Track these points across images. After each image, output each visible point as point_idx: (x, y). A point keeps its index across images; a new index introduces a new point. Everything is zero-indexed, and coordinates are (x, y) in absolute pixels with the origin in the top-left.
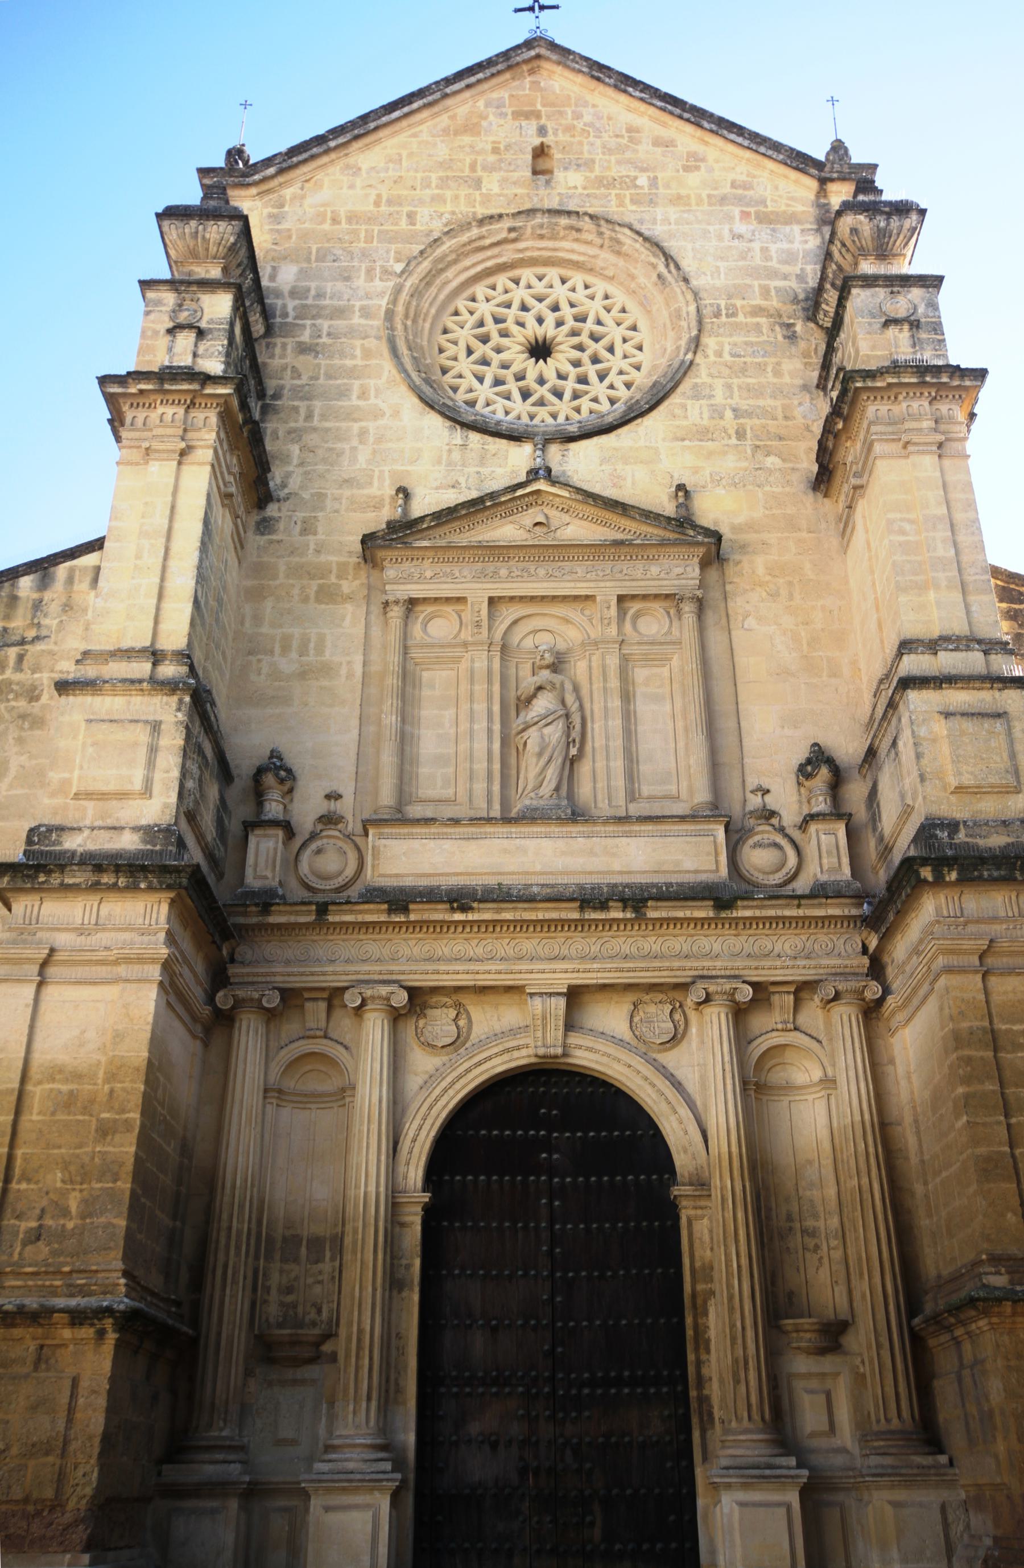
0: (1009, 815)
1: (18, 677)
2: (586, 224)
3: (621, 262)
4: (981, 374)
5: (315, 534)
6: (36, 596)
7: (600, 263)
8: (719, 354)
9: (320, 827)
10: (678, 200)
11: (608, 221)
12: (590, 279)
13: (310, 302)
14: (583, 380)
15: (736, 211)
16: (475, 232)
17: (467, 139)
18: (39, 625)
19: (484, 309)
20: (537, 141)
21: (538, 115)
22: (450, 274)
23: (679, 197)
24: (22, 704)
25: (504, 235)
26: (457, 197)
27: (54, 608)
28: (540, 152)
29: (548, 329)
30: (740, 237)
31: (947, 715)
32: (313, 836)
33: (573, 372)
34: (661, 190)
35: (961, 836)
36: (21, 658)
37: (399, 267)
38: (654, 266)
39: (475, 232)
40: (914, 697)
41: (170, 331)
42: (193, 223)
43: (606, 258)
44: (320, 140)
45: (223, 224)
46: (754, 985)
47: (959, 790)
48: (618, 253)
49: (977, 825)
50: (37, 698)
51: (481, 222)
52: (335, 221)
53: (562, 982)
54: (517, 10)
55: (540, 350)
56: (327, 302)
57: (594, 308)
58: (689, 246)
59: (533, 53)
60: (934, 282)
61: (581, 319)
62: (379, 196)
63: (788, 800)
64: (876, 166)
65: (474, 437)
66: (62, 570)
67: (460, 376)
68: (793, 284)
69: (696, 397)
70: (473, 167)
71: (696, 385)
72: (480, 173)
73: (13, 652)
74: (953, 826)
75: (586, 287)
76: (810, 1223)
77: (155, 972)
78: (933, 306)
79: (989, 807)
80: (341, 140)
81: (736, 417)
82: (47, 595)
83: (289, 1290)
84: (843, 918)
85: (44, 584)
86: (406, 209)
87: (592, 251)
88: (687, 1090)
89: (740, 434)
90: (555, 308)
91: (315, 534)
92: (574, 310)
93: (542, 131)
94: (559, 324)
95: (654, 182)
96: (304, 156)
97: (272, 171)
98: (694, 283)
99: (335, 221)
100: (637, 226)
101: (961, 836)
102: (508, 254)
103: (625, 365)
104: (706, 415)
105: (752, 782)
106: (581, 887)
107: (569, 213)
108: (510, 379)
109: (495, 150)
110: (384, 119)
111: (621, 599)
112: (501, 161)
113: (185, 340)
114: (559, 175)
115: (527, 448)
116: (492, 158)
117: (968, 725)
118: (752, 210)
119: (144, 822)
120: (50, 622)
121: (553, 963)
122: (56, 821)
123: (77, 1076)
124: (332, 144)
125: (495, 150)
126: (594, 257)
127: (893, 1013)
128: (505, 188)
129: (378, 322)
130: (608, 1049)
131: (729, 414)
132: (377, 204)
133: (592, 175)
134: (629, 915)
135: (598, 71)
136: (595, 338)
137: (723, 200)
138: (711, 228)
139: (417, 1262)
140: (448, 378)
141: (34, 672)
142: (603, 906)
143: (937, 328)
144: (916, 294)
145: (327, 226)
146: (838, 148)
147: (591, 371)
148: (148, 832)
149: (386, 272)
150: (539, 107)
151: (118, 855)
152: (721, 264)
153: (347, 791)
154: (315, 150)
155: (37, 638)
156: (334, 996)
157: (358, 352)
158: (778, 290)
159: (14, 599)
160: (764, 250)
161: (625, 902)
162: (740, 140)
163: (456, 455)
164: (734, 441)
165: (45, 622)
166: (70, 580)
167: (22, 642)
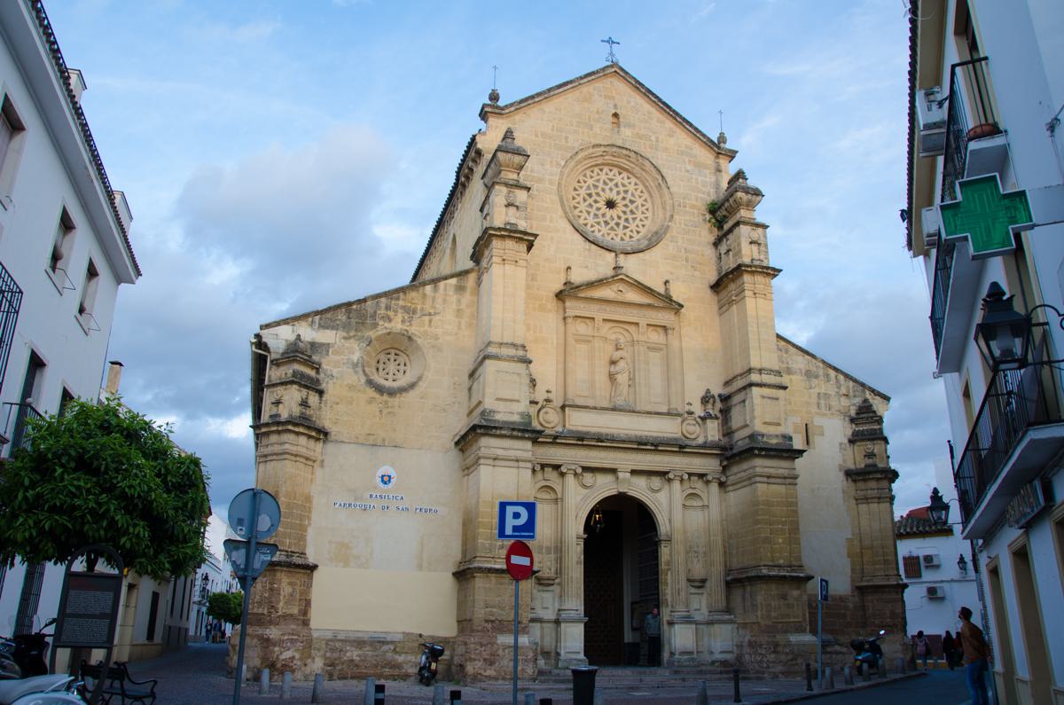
0: (777, 433)
1: (429, 329)
2: (632, 155)
3: (643, 173)
4: (780, 271)
5: (536, 281)
6: (433, 295)
8: (680, 224)
9: (545, 403)
10: (666, 150)
11: (641, 156)
12: (649, 200)
13: (528, 173)
14: (627, 220)
15: (687, 160)
16: (591, 150)
17: (586, 105)
18: (435, 307)
19: (590, 182)
20: (614, 111)
21: (613, 98)
22: (579, 166)
23: (667, 149)
25: (601, 153)
26: (583, 132)
27: (439, 300)
29: (617, 199)
30: (688, 171)
31: (763, 397)
32: (543, 407)
33: (623, 217)
34: (660, 144)
35: (765, 439)
36: (430, 321)
37: (563, 163)
38: (658, 180)
39: (591, 150)
40: (754, 389)
41: (506, 206)
42: (510, 155)
43: (637, 170)
44: (532, 97)
45: (521, 157)
46: (688, 474)
47: (765, 423)
48: (643, 170)
49: (770, 436)
51: (594, 146)
52: (536, 136)
53: (630, 468)
54: (602, 41)
55: (611, 204)
56: (535, 175)
57: (639, 202)
58: (670, 172)
59: (613, 70)
60: (765, 227)
61: (632, 202)
62: (553, 126)
63: (699, 410)
64: (736, 152)
65: (593, 246)
66: (442, 284)
67: (581, 212)
68: (706, 196)
69: (672, 241)
70: (589, 120)
71: (672, 237)
72: (592, 123)
73: (427, 318)
74: (763, 436)
75: (642, 192)
76: (695, 549)
77: (530, 465)
78: (765, 237)
79: (772, 430)
80: (540, 98)
81: (686, 252)
82: (437, 295)
83: (540, 563)
84: (718, 454)
85: (436, 289)
86: (564, 135)
87: (633, 166)
89: (687, 260)
91: (536, 281)
92: (624, 189)
93: (615, 106)
94: (624, 199)
95: (657, 138)
96: (525, 104)
97: (513, 109)
98: (672, 190)
99: (536, 136)
100: (651, 160)
101: (765, 439)
102: (600, 161)
103: (642, 216)
104: (676, 250)
105: (687, 401)
106: (636, 436)
107: (626, 149)
108: (594, 208)
109: (598, 112)
110: (557, 91)
111: (648, 325)
112: (600, 118)
113: (512, 210)
114: (622, 129)
115: (613, 254)
116: (597, 116)
117: (769, 401)
118: (692, 160)
119: (520, 411)
120: (439, 306)
121: (625, 461)
122: (496, 410)
124: (537, 100)
125: (598, 112)
126: (633, 168)
127: (728, 486)
128: (602, 132)
129: (555, 188)
130: (639, 489)
131: (683, 250)
132: (553, 130)
133: (635, 132)
134: (653, 448)
135: (638, 86)
136: (632, 202)
137: (682, 153)
138: (678, 166)
139: (582, 557)
140: (576, 212)
141: (436, 328)
142: (646, 444)
143: (766, 246)
144: (760, 230)
145: (533, 137)
146: (722, 139)
147: (630, 217)
148: (522, 414)
149: (558, 164)
150: (614, 95)
151: (513, 423)
152: (682, 183)
153: (553, 389)
154: (529, 102)
155: (435, 314)
156: (556, 467)
157: (548, 200)
158: (701, 198)
159: (425, 295)
160: (696, 179)
161: (652, 444)
162: (690, 129)
163: (586, 253)
164: (684, 263)
165: (437, 306)
166: (445, 290)
167: (430, 314)
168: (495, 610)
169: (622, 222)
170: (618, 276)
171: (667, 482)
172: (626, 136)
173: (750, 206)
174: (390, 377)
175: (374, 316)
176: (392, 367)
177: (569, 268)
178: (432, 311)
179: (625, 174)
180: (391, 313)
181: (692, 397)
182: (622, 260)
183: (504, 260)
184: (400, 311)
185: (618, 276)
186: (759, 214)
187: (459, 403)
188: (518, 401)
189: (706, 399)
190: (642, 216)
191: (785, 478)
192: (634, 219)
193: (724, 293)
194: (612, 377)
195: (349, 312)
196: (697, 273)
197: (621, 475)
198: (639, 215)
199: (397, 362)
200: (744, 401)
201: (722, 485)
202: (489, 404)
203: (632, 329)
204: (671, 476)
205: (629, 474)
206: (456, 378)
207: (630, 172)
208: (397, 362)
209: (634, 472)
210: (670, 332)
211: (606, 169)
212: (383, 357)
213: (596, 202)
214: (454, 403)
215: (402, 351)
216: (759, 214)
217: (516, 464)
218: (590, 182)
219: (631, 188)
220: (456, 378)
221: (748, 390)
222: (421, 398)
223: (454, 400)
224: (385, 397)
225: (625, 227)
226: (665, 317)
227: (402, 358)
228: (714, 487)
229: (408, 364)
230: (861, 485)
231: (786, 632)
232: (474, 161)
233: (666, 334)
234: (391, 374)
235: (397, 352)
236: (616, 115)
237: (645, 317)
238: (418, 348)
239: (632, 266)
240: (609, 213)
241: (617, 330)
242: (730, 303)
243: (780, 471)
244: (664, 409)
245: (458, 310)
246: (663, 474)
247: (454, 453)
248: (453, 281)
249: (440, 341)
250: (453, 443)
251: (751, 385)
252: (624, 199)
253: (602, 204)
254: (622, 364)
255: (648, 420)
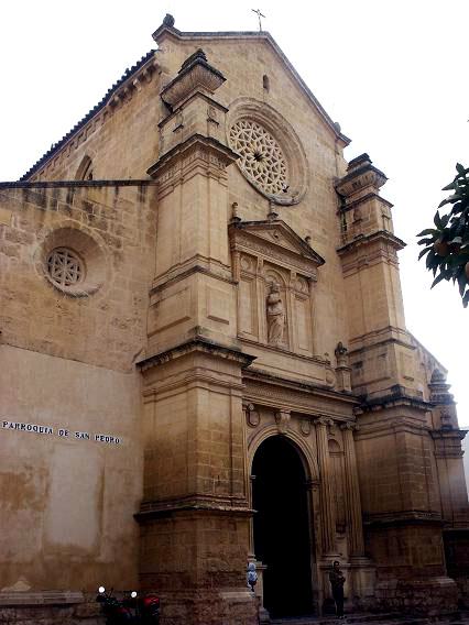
4: (405, 245)
7: (278, 133)
24: (114, 247)
28: (265, 78)
39: (248, 102)
48: (285, 133)
50: (119, 246)
51: (250, 99)
63: (332, 358)
88: (321, 453)
90: (269, 150)
123: (221, 428)
130: (293, 431)
165: (119, 211)
168: (217, 559)
169: (260, 175)
170: (271, 223)
171: (313, 427)
172: (273, 98)
173: (377, 185)
174: (63, 279)
175: (54, 205)
176: (65, 269)
177: (236, 204)
178: (114, 215)
179: (267, 134)
180: (73, 207)
181: (326, 349)
182: (275, 209)
183: (208, 173)
184: (81, 205)
185: (271, 223)
186: (384, 192)
187: (140, 320)
188: (227, 323)
189: (339, 351)
190: (280, 175)
191: (421, 429)
192: (276, 176)
193: (347, 260)
194: (271, 319)
195: (26, 192)
196: (326, 237)
197: (283, 415)
198: (278, 173)
199: (71, 264)
200: (384, 355)
201: (355, 432)
202: (201, 320)
203: (283, 275)
204: (321, 420)
205: (288, 416)
206: (137, 293)
207: (275, 135)
208: (71, 264)
209: (292, 413)
210: (313, 284)
211: (254, 124)
212: (56, 256)
213: (247, 152)
214: (135, 320)
215: (77, 253)
216: (384, 192)
217: (226, 391)
218: (242, 131)
219: (273, 148)
220: (137, 293)
221: (388, 346)
222: (103, 308)
223: (135, 316)
224: (64, 300)
225: (269, 182)
226: (307, 271)
227: (76, 261)
228: (350, 435)
229: (82, 268)
230: (438, 442)
231: (433, 575)
232: (142, 79)
233: (309, 286)
234: (64, 275)
235: (73, 254)
236: (265, 78)
237: (294, 267)
238: (98, 251)
239: (282, 214)
240: (258, 164)
241: (272, 274)
242: (362, 265)
243: (419, 423)
244: (311, 355)
245: (140, 221)
246: (313, 420)
247: (135, 375)
248: (135, 189)
249: (121, 249)
250: (134, 364)
251: (394, 340)
252: (267, 155)
253: (251, 155)
254: (280, 307)
255: (303, 364)
